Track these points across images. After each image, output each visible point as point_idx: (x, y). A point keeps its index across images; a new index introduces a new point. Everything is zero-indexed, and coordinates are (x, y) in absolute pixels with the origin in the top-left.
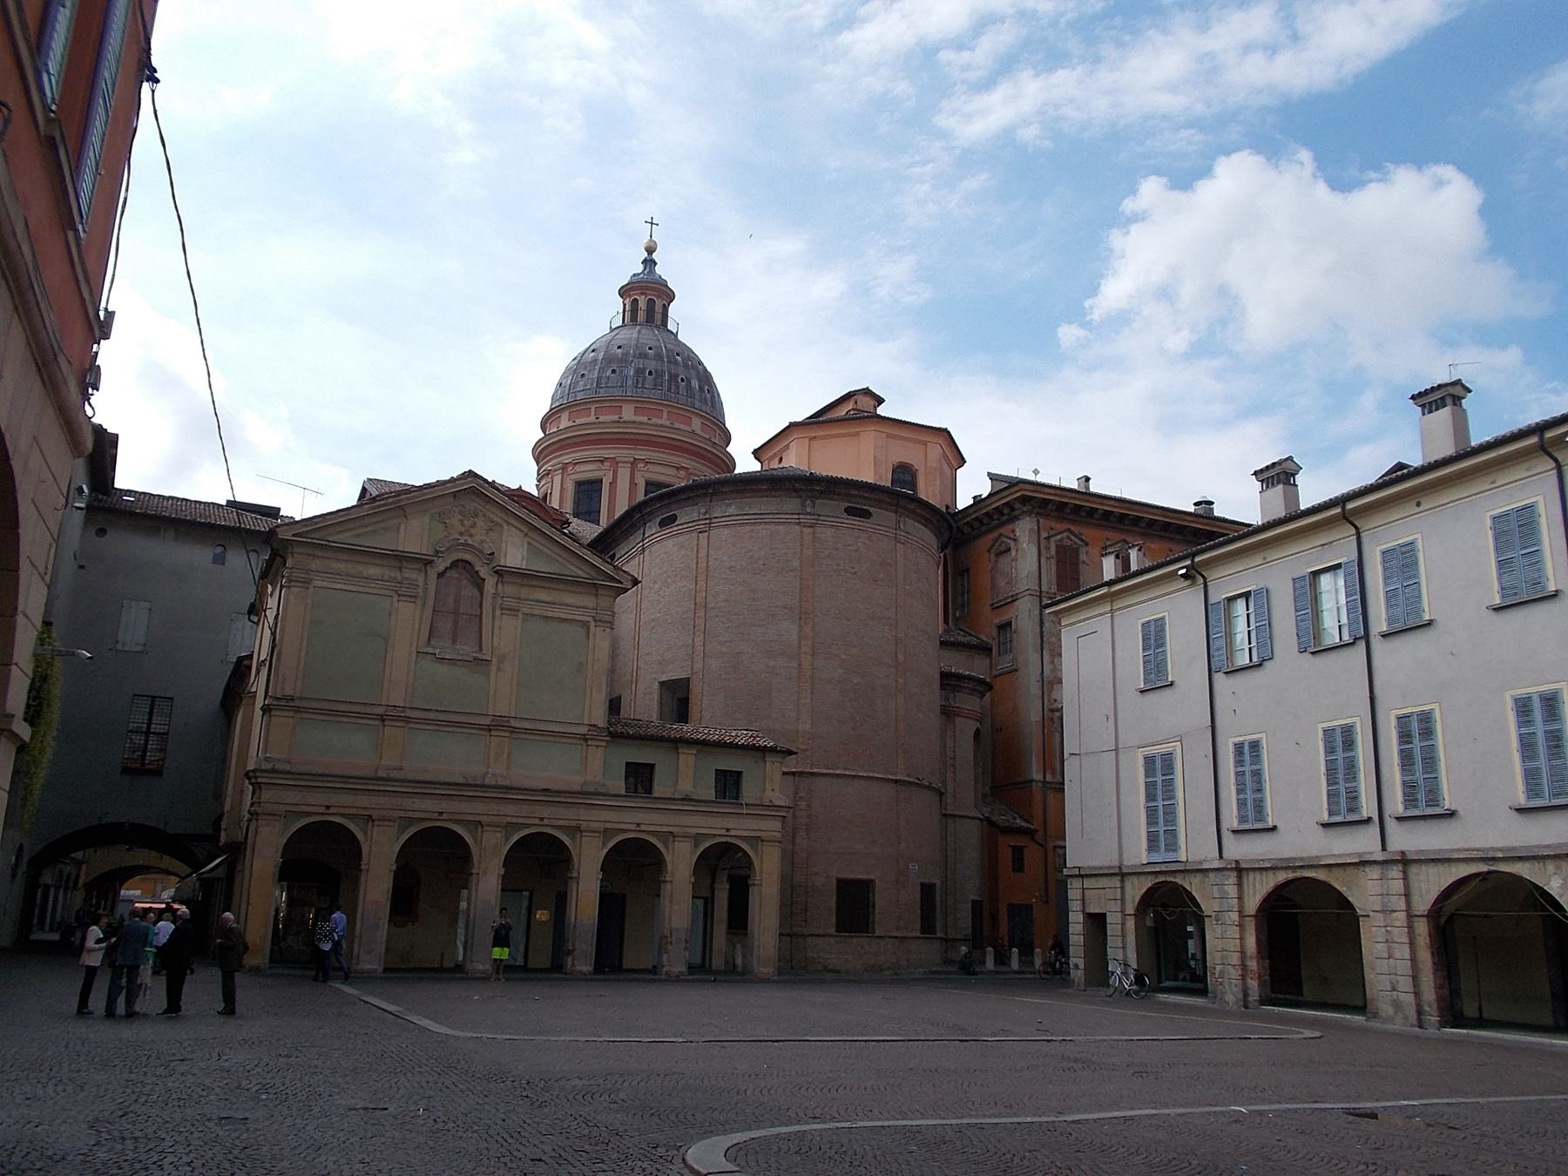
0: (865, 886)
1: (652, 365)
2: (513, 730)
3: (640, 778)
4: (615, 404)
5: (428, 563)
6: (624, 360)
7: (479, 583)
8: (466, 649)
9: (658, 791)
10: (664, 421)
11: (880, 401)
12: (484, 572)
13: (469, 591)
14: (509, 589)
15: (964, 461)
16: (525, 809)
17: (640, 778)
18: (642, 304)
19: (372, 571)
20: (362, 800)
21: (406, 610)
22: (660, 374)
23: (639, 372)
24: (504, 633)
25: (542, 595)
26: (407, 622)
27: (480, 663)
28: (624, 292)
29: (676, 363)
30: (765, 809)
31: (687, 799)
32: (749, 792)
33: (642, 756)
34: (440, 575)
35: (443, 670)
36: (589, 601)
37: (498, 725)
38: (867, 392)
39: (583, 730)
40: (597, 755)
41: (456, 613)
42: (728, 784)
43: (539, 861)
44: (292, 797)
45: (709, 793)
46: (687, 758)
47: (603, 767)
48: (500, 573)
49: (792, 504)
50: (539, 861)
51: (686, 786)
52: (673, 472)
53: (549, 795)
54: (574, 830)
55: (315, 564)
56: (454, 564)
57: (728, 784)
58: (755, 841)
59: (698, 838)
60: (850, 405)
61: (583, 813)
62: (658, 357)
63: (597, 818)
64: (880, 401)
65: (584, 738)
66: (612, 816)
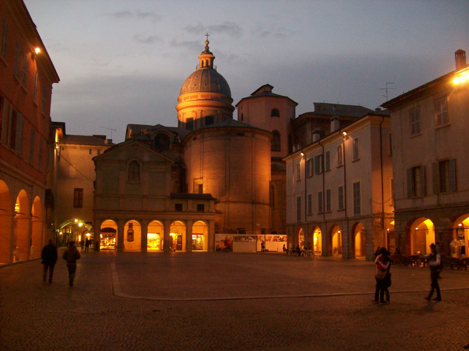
7: (139, 166)
9: (183, 210)
11: (272, 87)
15: (297, 104)
31: (190, 212)
32: (206, 209)
33: (179, 202)
34: (130, 164)
38: (268, 85)
39: (164, 197)
45: (196, 210)
46: (190, 202)
48: (143, 163)
56: (133, 162)
60: (263, 90)
64: (272, 87)
66: (173, 216)
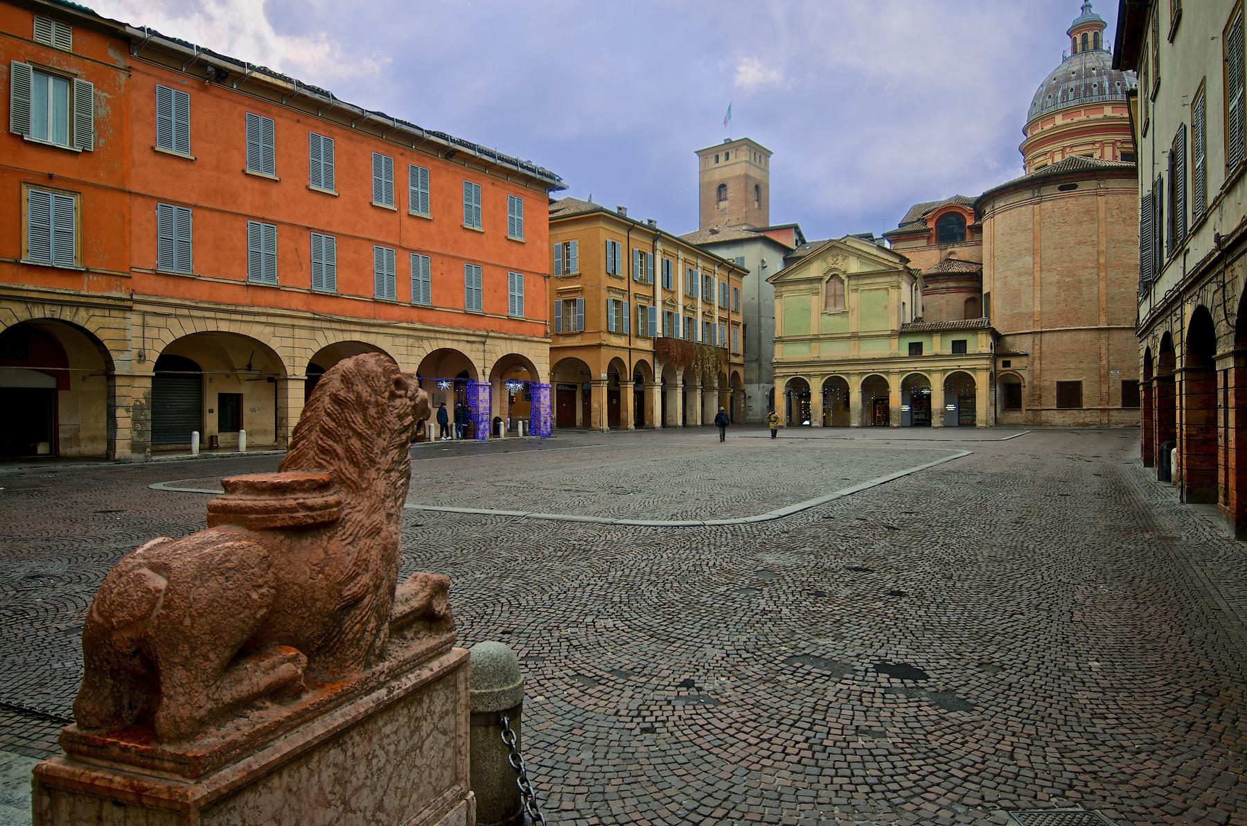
0: (1078, 385)
1: (1072, 84)
2: (859, 337)
3: (916, 349)
4: (1051, 117)
5: (820, 279)
6: (1057, 88)
7: (842, 282)
8: (839, 309)
10: (1083, 118)
12: (843, 277)
13: (839, 286)
14: (853, 282)
16: (866, 367)
17: (916, 349)
18: (1079, 41)
19: (802, 287)
20: (807, 369)
21: (815, 298)
22: (1078, 88)
23: (1065, 92)
24: (853, 299)
25: (868, 281)
26: (816, 302)
27: (845, 313)
28: (1069, 34)
29: (1091, 76)
30: (980, 356)
31: (936, 355)
32: (970, 349)
35: (832, 318)
36: (888, 279)
37: (855, 337)
40: (895, 342)
41: (835, 295)
42: (959, 347)
43: (875, 388)
44: (785, 370)
45: (949, 351)
46: (937, 339)
47: (900, 348)
48: (850, 277)
49: (1027, 195)
50: (875, 388)
51: (937, 349)
52: (1090, 147)
53: (875, 361)
54: (887, 373)
55: (784, 289)
57: (959, 347)
58: (974, 370)
59: (945, 371)
61: (891, 366)
62: (1079, 77)
63: (896, 367)
65: (889, 336)
